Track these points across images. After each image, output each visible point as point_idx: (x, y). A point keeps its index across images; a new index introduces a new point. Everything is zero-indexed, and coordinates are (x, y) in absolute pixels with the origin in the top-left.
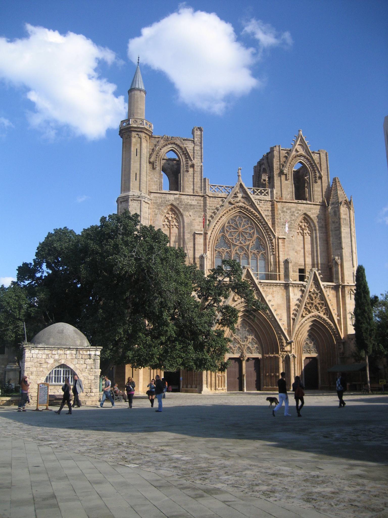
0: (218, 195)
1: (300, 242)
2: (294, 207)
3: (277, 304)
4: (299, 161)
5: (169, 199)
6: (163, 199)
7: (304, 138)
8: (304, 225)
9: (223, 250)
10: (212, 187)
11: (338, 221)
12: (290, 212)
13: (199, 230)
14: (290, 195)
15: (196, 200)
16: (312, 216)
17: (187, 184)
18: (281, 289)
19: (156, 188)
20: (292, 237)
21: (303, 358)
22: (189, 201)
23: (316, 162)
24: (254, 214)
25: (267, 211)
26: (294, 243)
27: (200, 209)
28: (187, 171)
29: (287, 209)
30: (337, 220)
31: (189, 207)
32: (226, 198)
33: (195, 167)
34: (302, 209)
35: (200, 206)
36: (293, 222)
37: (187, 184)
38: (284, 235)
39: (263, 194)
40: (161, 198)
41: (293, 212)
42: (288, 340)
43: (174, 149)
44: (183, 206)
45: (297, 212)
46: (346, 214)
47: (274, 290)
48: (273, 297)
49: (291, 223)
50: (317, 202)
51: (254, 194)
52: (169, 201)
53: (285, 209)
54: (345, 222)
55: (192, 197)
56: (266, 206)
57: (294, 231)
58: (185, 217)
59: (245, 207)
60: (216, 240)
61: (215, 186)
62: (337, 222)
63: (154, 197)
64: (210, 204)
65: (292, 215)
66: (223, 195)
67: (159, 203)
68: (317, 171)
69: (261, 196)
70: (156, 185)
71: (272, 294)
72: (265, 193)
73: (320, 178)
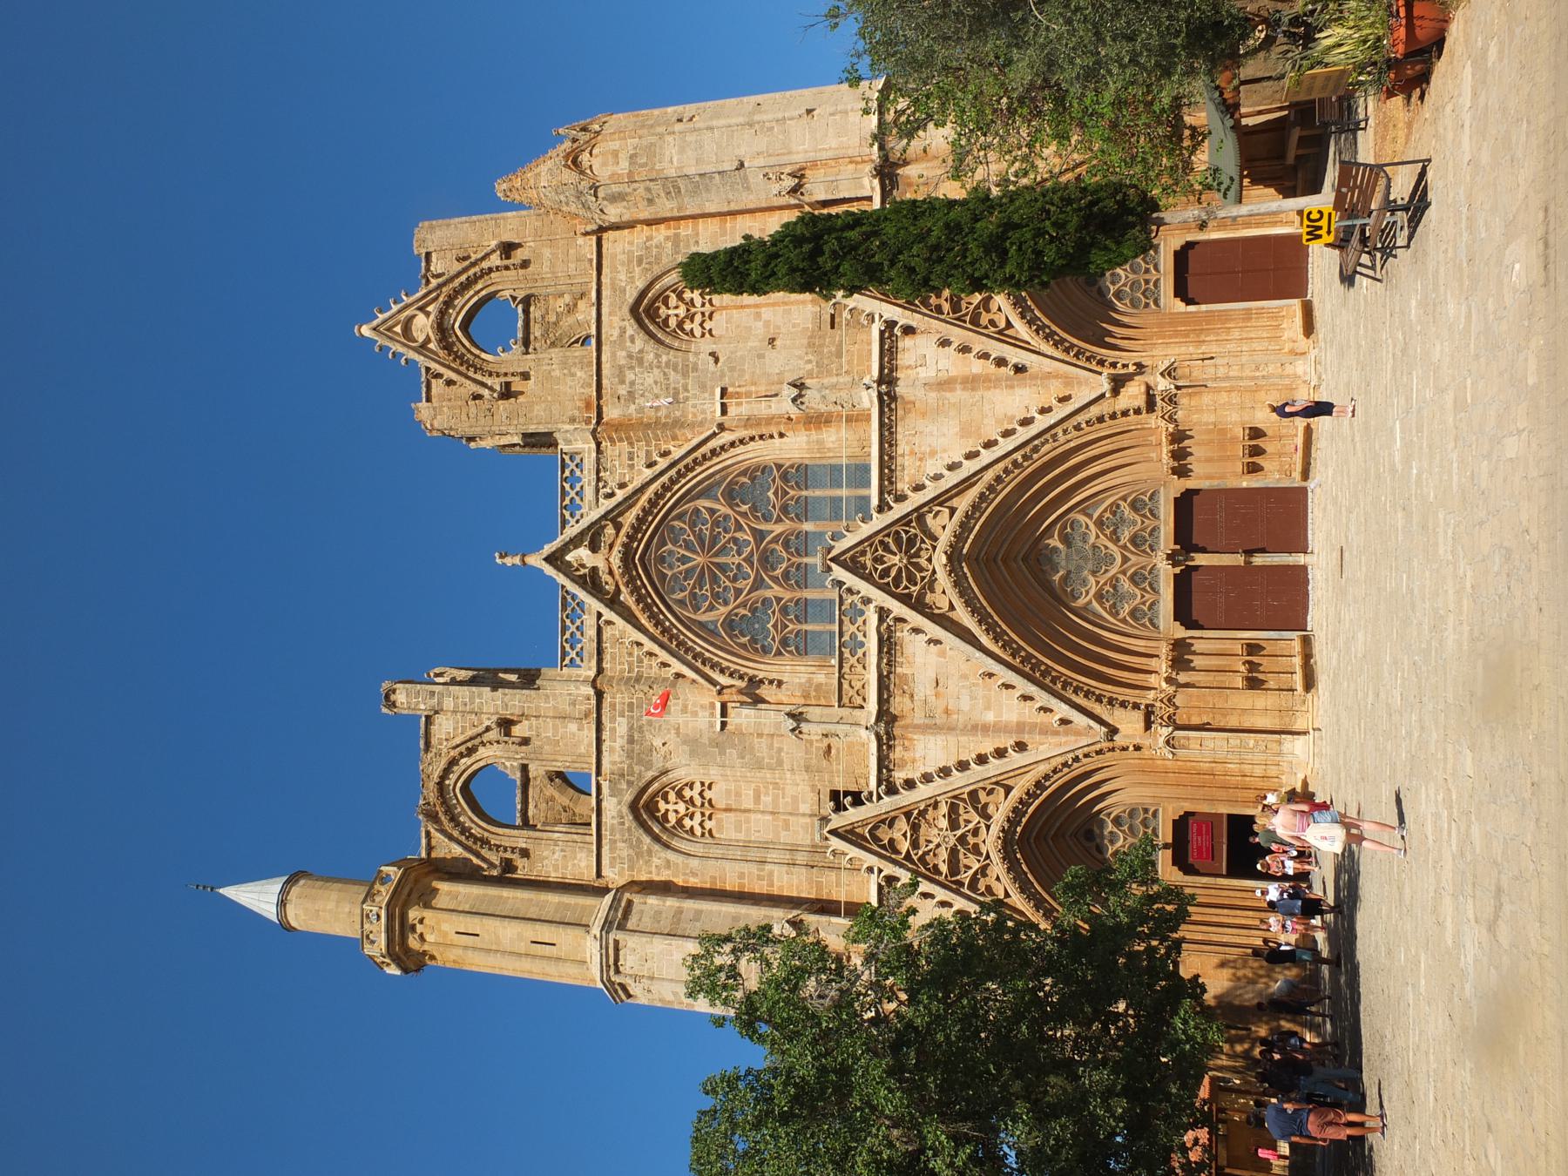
0: (591, 640)
1: (738, 326)
2: (614, 355)
3: (962, 437)
4: (459, 333)
5: (615, 814)
6: (618, 836)
7: (381, 317)
8: (677, 307)
9: (775, 626)
10: (567, 661)
11: (642, 185)
12: (631, 368)
13: (712, 715)
14: (573, 370)
15: (613, 720)
16: (641, 284)
17: (566, 745)
18: (902, 419)
19: (584, 855)
20: (717, 360)
21: (1180, 306)
22: (617, 745)
23: (458, 267)
24: (644, 510)
25: (631, 459)
26: (739, 354)
27: (640, 707)
28: (525, 741)
29: (622, 382)
30: (641, 191)
31: (637, 747)
32: (599, 615)
33: (507, 714)
34: (616, 319)
35: (631, 705)
36: (664, 358)
37: (566, 745)
38: (713, 394)
39: (578, 473)
40: (613, 842)
41: (630, 356)
42: (1102, 396)
43: (459, 785)
44: (636, 769)
45: (628, 344)
46: (615, 154)
47: (907, 449)
48: (933, 453)
49: (668, 364)
50: (591, 260)
51: (580, 507)
52: (622, 817)
53: (623, 390)
54: (644, 160)
55: (606, 735)
56: (617, 463)
57: (697, 354)
58: (669, 765)
59: (624, 545)
60: (743, 652)
61: (563, 648)
62: (648, 190)
63: (612, 866)
64: (622, 671)
65: (640, 361)
66: (589, 621)
67: (631, 851)
68: (485, 265)
69: (585, 480)
70: (574, 852)
71: (921, 460)
72: (572, 466)
73: (508, 249)
